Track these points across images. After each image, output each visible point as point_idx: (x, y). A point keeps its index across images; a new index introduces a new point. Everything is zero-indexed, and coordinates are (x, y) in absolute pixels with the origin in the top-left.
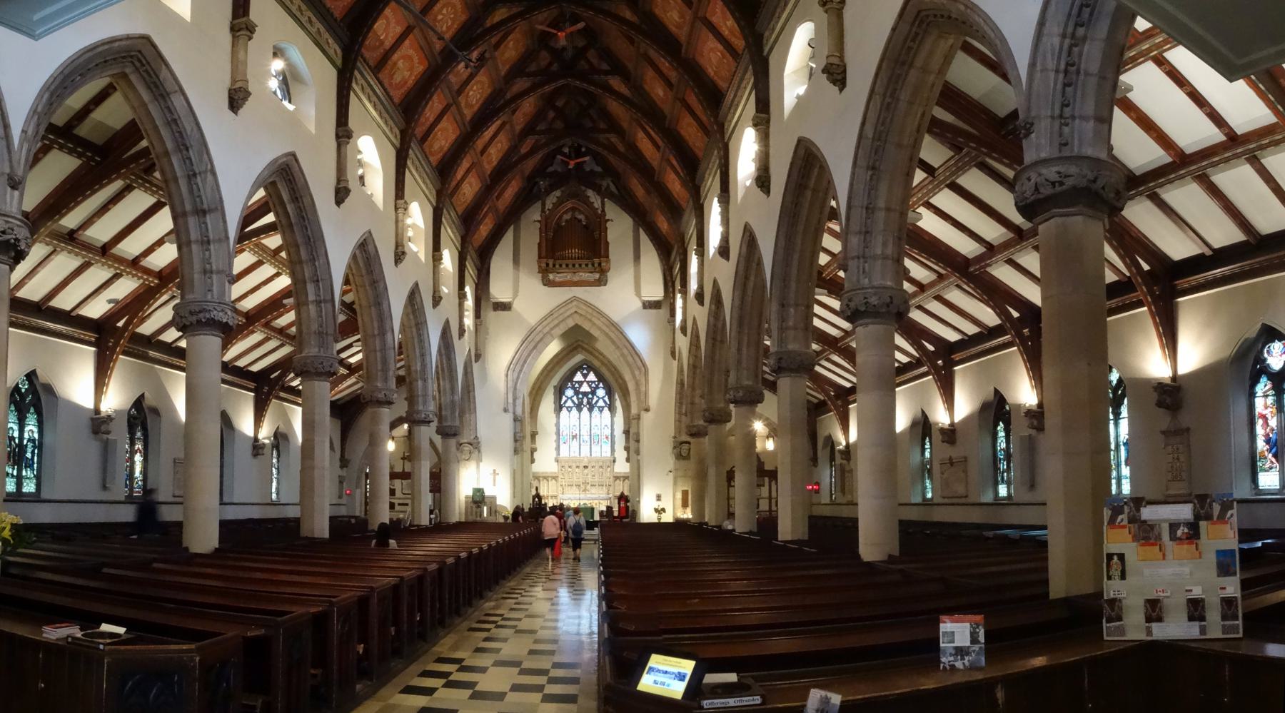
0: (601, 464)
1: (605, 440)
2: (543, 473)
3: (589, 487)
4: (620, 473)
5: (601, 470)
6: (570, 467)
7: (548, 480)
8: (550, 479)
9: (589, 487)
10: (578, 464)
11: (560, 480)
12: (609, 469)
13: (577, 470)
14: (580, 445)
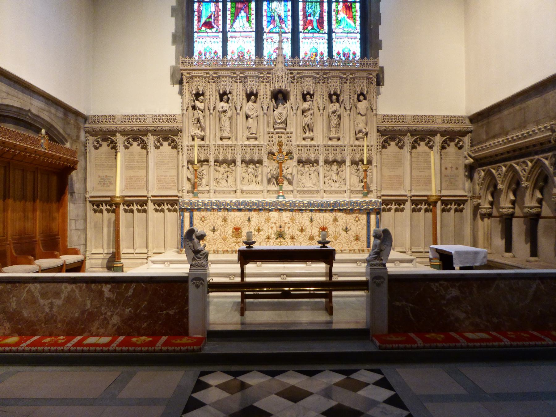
0: (334, 85)
1: (342, 15)
2: (128, 118)
3: (291, 167)
4: (401, 119)
5: (335, 106)
6: (223, 96)
7: (145, 147)
8: (151, 140)
9: (291, 167)
10: (252, 85)
11: (186, 141)
12: (362, 106)
13: (249, 107)
14: (259, 32)
